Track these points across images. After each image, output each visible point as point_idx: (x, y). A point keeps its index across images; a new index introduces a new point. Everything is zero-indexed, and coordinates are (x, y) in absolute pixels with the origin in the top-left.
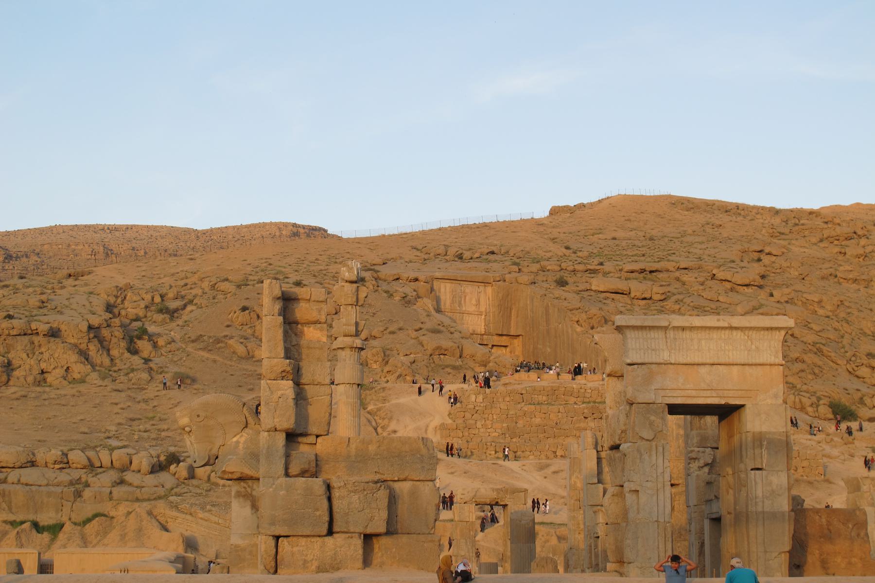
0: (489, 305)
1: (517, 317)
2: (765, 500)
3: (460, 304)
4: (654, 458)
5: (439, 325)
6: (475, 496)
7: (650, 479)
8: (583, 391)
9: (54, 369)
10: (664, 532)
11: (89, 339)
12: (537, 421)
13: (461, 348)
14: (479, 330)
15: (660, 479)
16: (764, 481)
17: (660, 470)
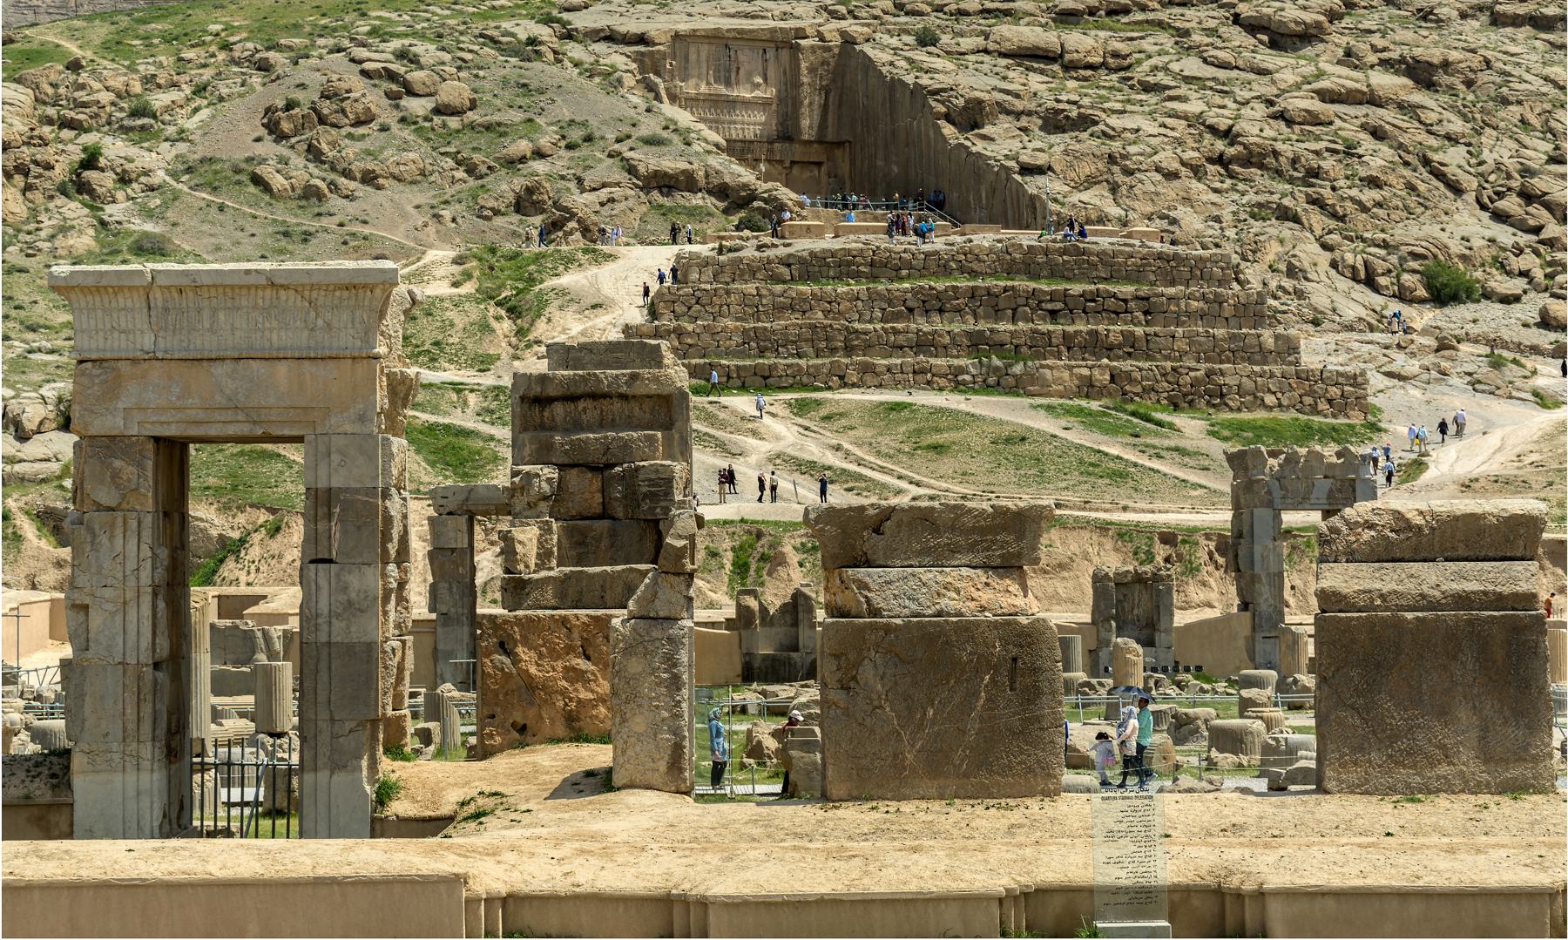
0: (786, 84)
2: (334, 620)
4: (119, 541)
5: (666, 128)
6: (467, 499)
7: (109, 581)
10: (136, 685)
15: (132, 582)
16: (333, 584)
17: (131, 564)
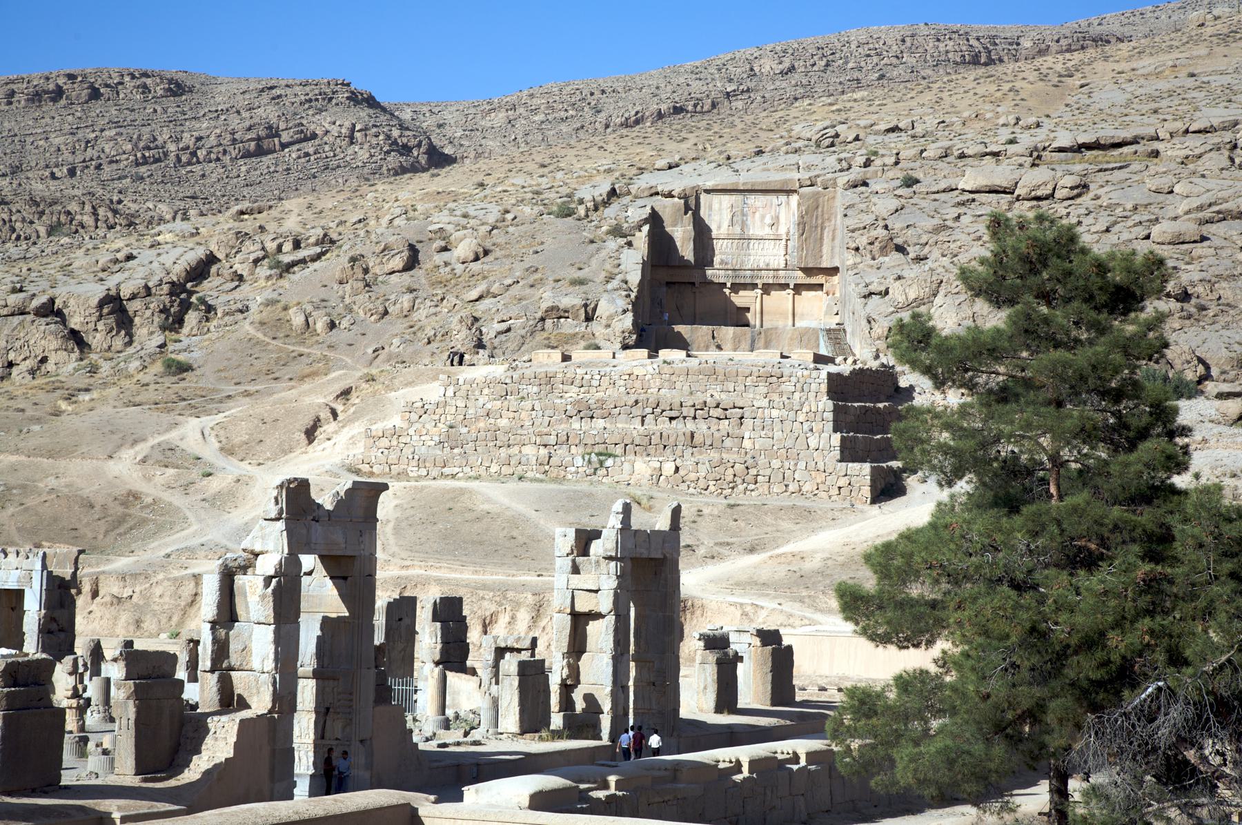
1: (833, 239)
3: (744, 225)
8: (588, 377)
9: (25, 359)
11: (101, 316)
12: (503, 422)
13: (590, 309)
14: (776, 263)
